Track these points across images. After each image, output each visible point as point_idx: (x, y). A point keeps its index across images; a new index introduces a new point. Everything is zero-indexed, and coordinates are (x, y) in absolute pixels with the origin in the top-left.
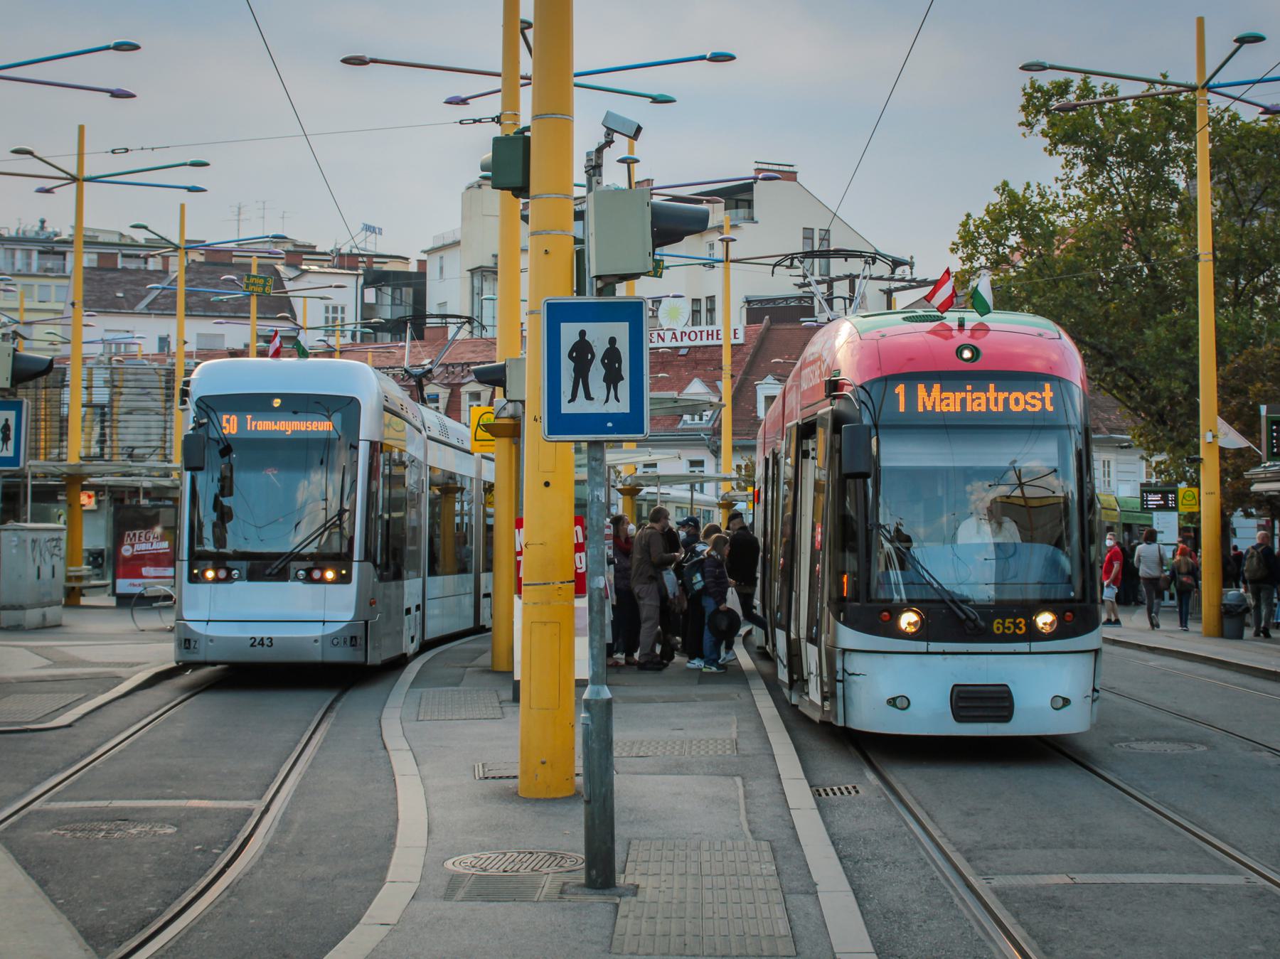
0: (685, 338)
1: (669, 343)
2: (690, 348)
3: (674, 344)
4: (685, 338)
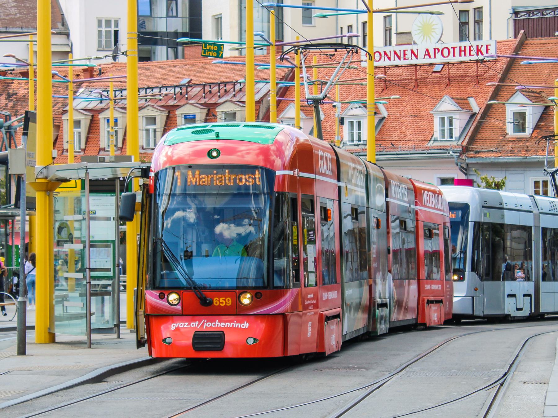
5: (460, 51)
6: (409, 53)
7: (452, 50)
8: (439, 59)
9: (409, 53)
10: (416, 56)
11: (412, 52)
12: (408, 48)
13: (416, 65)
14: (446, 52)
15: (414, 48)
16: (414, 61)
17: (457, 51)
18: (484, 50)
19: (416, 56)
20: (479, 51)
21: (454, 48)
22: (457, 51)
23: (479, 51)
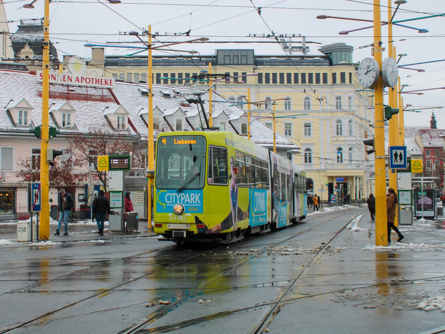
0: (84, 81)
1: (74, 83)
4: (84, 81)
5: (96, 81)
7: (91, 80)
10: (71, 81)
11: (69, 77)
14: (88, 80)
17: (94, 80)
18: (109, 82)
19: (71, 81)
20: (106, 82)
21: (93, 79)
22: (94, 80)
23: (106, 82)
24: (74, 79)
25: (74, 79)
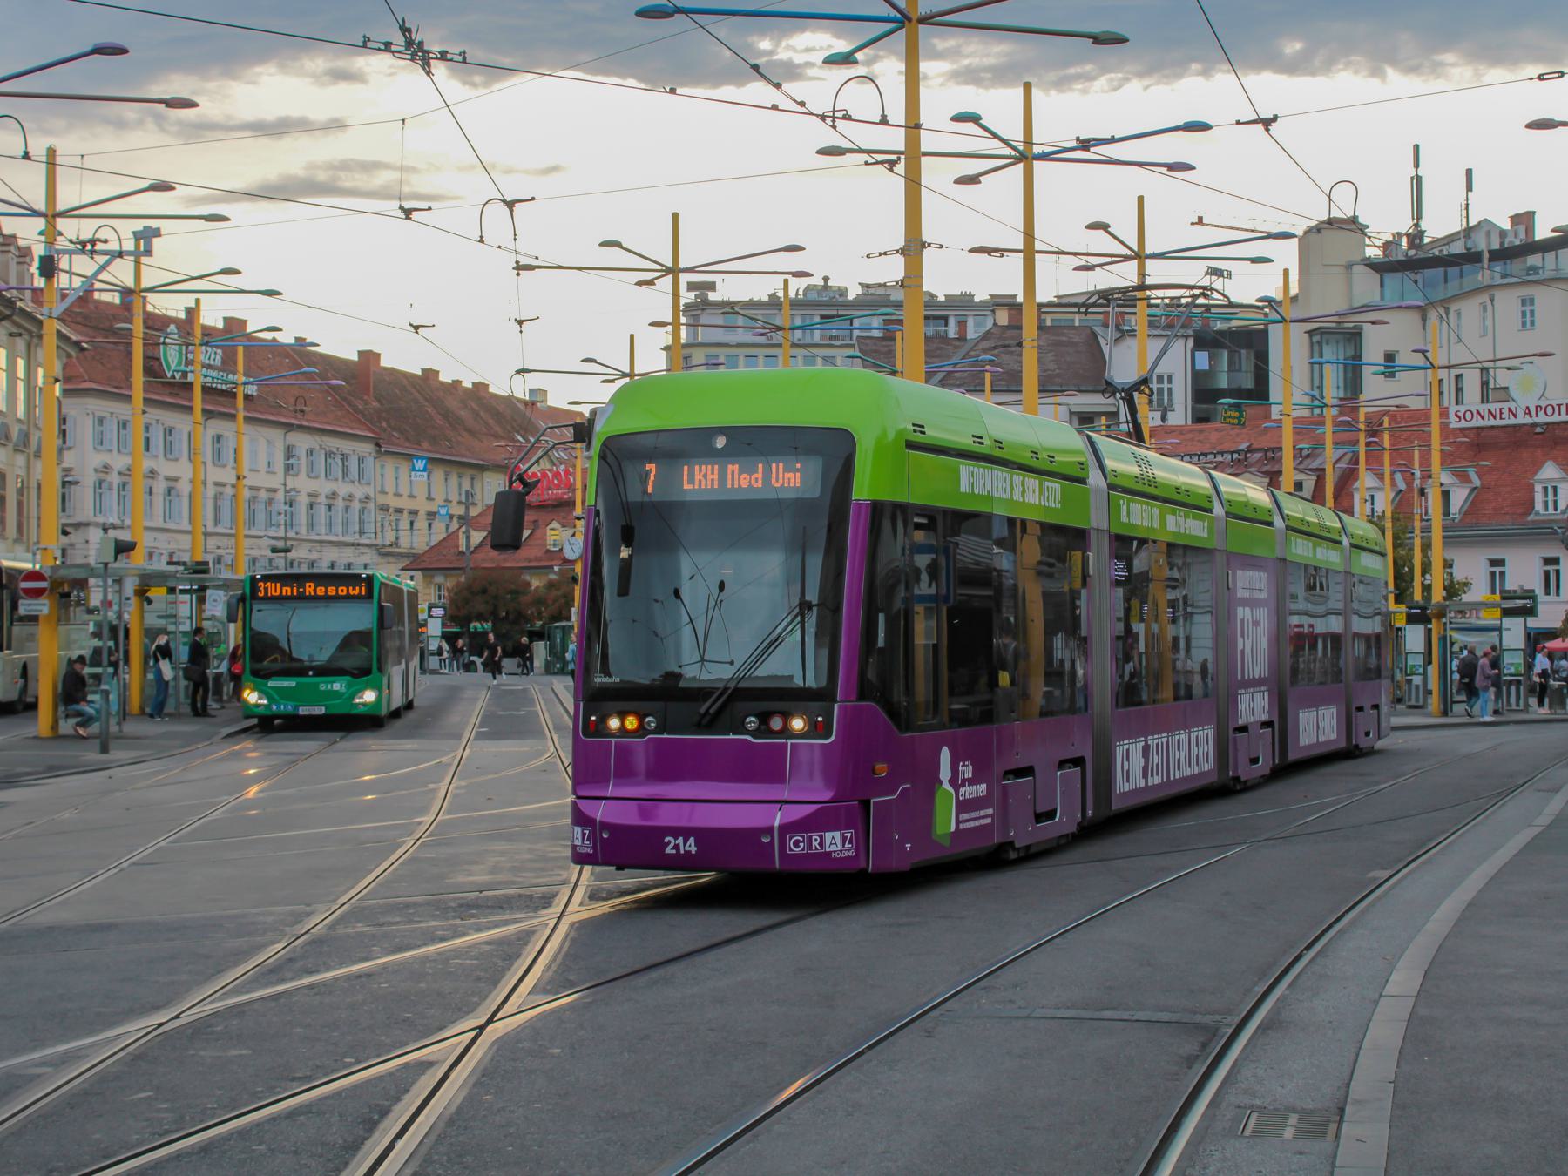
0: (1541, 414)
1: (1522, 419)
2: (1547, 424)
3: (1528, 420)
4: (1541, 414)
6: (1506, 411)
8: (1542, 418)
9: (1506, 411)
12: (1505, 406)
13: (1514, 426)
14: (1550, 410)
15: (1512, 405)
16: (1512, 421)
24: (1520, 413)
25: (1520, 413)
